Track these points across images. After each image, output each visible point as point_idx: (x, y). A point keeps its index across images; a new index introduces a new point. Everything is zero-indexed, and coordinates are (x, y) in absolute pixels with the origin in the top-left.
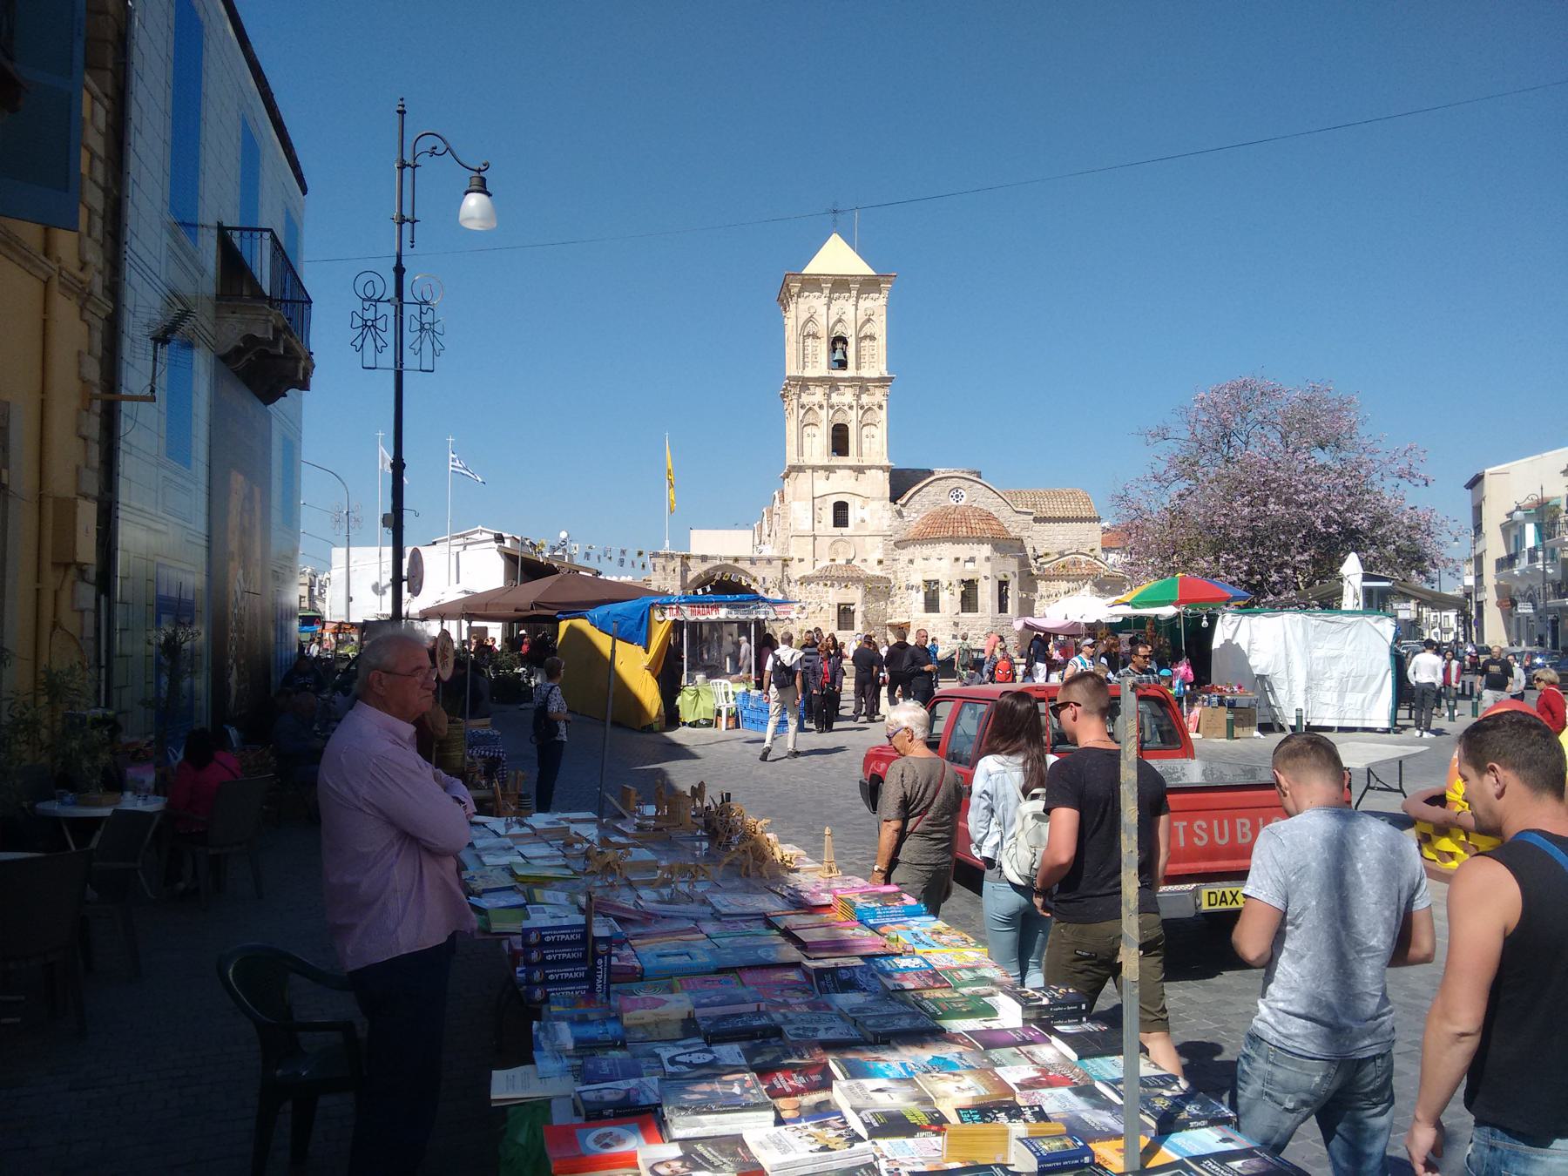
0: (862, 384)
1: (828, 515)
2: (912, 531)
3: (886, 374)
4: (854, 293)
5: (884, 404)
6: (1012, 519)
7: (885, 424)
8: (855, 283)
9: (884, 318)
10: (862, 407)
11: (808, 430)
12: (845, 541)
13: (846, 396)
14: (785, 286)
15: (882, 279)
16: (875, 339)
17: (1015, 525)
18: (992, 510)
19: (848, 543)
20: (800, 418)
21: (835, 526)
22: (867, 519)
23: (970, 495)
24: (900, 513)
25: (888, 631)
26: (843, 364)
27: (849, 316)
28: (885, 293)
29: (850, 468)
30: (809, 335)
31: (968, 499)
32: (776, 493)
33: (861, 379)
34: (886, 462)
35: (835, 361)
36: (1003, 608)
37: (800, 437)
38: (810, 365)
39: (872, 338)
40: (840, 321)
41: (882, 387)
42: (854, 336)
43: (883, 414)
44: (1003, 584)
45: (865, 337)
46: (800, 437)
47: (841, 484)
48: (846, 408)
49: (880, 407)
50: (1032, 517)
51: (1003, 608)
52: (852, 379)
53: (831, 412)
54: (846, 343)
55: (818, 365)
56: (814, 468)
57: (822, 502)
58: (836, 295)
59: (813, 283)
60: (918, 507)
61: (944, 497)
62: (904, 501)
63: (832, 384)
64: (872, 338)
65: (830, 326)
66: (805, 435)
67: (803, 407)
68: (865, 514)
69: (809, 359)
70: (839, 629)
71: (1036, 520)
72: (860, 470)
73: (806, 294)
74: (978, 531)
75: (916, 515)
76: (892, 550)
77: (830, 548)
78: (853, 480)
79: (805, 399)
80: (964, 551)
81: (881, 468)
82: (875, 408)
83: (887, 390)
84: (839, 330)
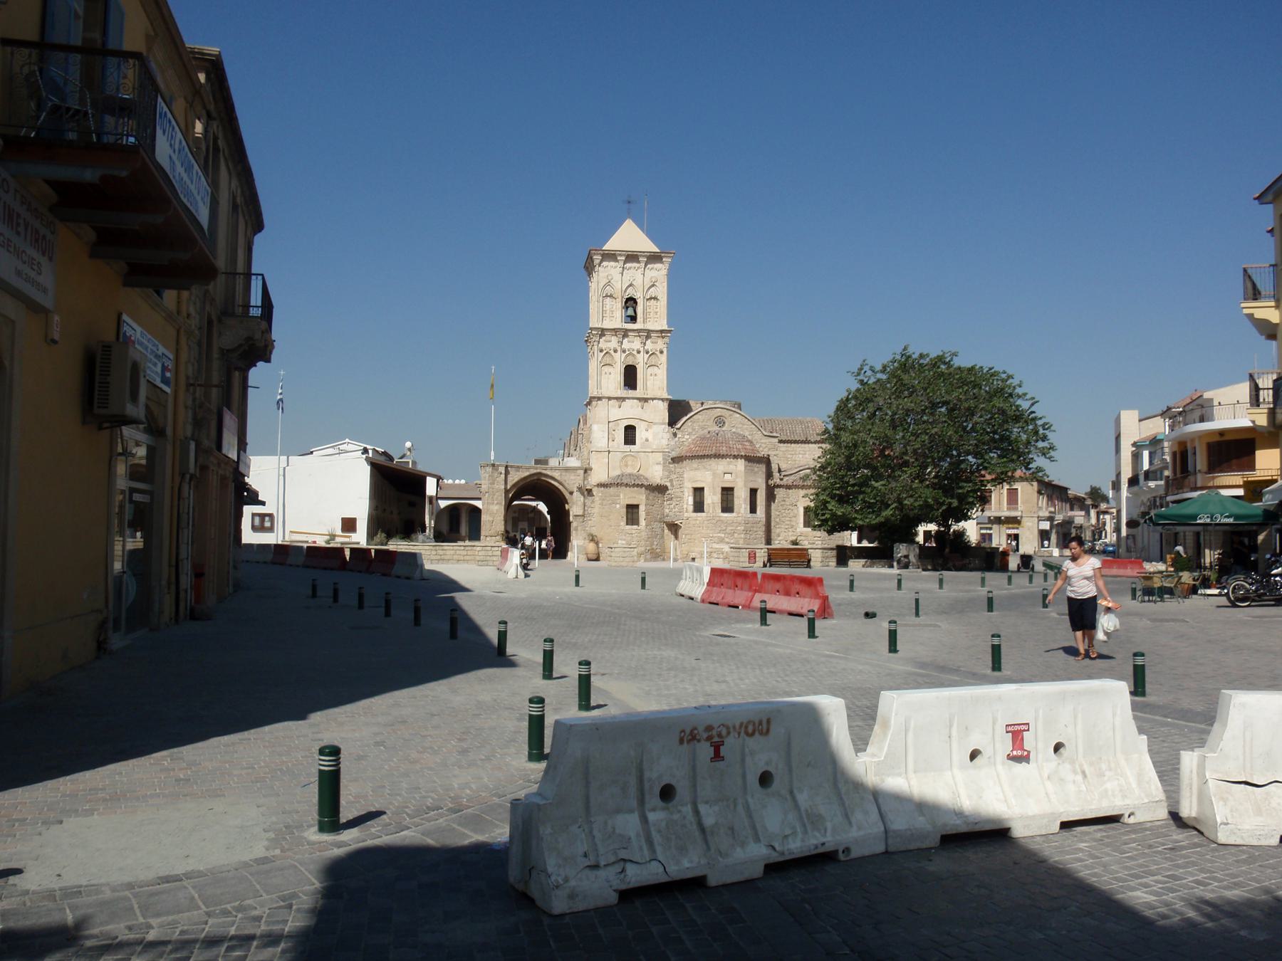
0: (648, 334)
1: (620, 435)
3: (666, 328)
6: (762, 441)
7: (665, 366)
10: (647, 353)
11: (606, 369)
12: (633, 456)
14: (590, 259)
15: (663, 255)
16: (658, 299)
17: (764, 446)
18: (747, 434)
24: (675, 435)
25: (665, 526)
26: (633, 319)
27: (638, 280)
28: (667, 265)
29: (639, 399)
30: (607, 296)
31: (729, 425)
33: (649, 332)
34: (666, 396)
35: (628, 316)
36: (753, 510)
37: (599, 374)
38: (608, 319)
39: (655, 298)
40: (631, 285)
41: (663, 337)
42: (642, 297)
43: (663, 358)
44: (753, 492)
45: (651, 298)
46: (599, 374)
47: (630, 411)
48: (635, 353)
49: (661, 352)
50: (776, 440)
51: (753, 510)
53: (624, 355)
55: (614, 319)
56: (610, 399)
58: (628, 265)
59: (611, 256)
60: (690, 430)
61: (711, 423)
62: (678, 426)
63: (625, 333)
64: (655, 298)
65: (624, 289)
67: (601, 351)
68: (649, 435)
70: (627, 524)
71: (781, 442)
75: (687, 437)
76: (669, 463)
77: (621, 461)
79: (603, 344)
80: (722, 465)
81: (663, 400)
82: (658, 353)
83: (666, 340)
84: (630, 292)
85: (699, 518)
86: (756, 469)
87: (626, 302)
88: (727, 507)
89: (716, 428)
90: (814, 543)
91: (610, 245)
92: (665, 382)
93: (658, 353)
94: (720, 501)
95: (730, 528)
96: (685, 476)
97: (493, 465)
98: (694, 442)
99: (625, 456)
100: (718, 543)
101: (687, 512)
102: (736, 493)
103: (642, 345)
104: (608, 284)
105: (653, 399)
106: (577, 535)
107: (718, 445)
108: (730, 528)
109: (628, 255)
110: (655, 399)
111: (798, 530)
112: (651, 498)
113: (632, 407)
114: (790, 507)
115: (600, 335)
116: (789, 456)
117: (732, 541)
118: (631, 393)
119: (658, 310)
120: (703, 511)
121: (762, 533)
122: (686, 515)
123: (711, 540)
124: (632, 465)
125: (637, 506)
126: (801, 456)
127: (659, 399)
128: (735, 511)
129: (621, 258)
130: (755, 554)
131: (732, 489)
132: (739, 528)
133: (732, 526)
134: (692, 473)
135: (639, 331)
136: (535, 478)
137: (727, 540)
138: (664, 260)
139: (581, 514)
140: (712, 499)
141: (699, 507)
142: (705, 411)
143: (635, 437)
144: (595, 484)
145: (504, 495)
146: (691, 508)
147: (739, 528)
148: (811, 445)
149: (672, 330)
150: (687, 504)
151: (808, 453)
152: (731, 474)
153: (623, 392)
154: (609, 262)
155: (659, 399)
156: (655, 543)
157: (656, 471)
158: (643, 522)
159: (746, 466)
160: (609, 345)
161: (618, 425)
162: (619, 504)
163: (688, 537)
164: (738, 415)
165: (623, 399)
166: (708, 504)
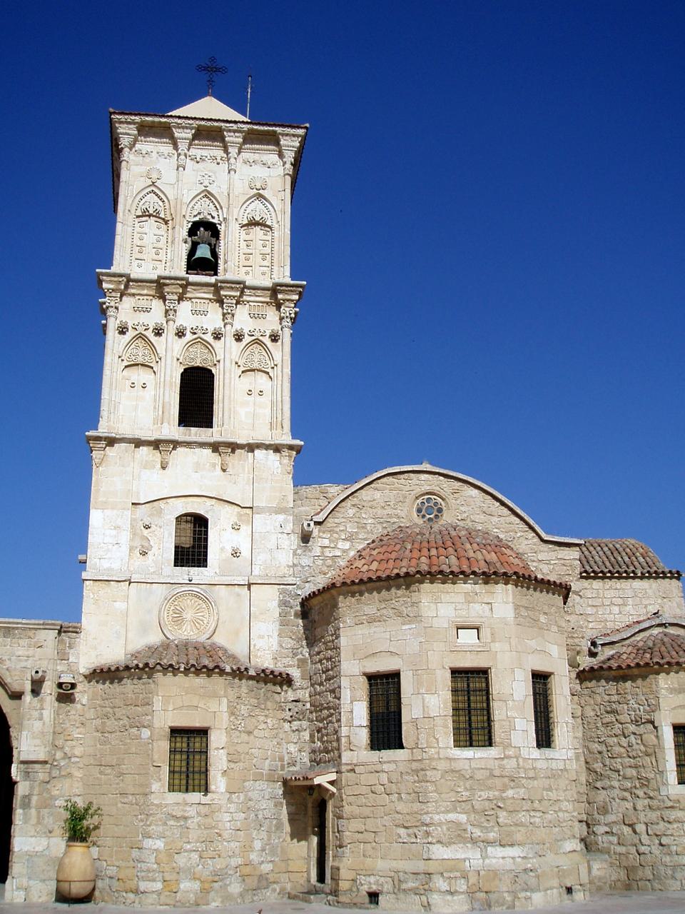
1: (165, 541)
7: (288, 370)
15: (279, 130)
19: (206, 600)
21: (175, 566)
26: (209, 266)
28: (290, 156)
29: (215, 447)
30: (146, 214)
34: (287, 439)
36: (544, 738)
43: (282, 353)
44: (541, 679)
45: (253, 223)
48: (209, 338)
50: (574, 554)
51: (544, 738)
56: (138, 443)
58: (196, 152)
60: (351, 528)
67: (122, 331)
75: (347, 545)
81: (277, 449)
82: (267, 340)
84: (205, 210)
85: (385, 767)
86: (543, 619)
87: (193, 231)
93: (267, 340)
95: (484, 795)
99: (177, 596)
102: (498, 686)
104: (153, 188)
105: (251, 448)
106: (26, 821)
107: (434, 552)
108: (484, 795)
110: (259, 446)
112: (244, 710)
113: (197, 467)
114: (632, 728)
116: (589, 610)
117: (492, 835)
118: (196, 434)
119: (267, 250)
120: (400, 746)
121: (570, 807)
122: (346, 757)
123: (428, 834)
124: (194, 622)
126: (616, 610)
127: (267, 447)
129: (184, 135)
132: (510, 793)
133: (490, 788)
134: (361, 630)
135: (216, 288)
137: (477, 833)
139: (42, 757)
142: (390, 479)
144: (87, 672)
146: (363, 736)
147: (510, 793)
148: (637, 584)
151: (630, 601)
153: (172, 430)
155: (267, 447)
156: (258, 845)
157: (261, 637)
158: (218, 782)
159: (517, 607)
160: (143, 318)
165: (176, 444)
166: (415, 722)
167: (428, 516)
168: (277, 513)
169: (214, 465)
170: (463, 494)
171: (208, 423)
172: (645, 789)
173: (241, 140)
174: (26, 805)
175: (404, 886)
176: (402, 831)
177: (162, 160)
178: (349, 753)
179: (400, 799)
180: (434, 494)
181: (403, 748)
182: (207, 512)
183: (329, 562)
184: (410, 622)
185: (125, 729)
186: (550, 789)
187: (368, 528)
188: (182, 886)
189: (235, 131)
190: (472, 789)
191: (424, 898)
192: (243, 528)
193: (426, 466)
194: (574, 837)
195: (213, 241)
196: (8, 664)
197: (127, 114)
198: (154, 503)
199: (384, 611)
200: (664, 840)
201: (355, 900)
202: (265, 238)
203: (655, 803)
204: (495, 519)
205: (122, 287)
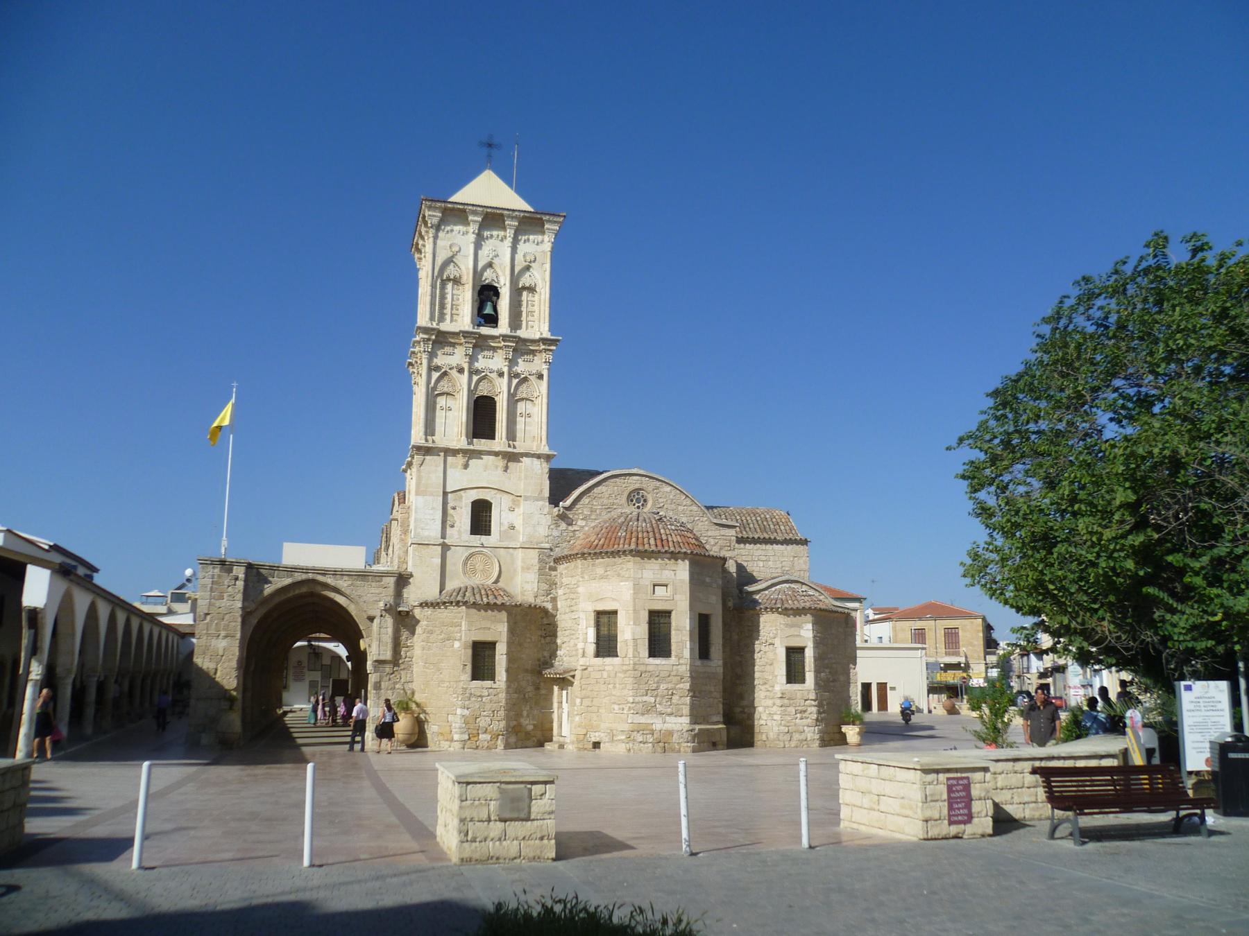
1: (463, 518)
2: (578, 544)
3: (547, 335)
4: (510, 233)
5: (545, 373)
6: (709, 533)
7: (545, 400)
8: (513, 218)
9: (548, 266)
13: (494, 362)
17: (717, 541)
18: (684, 520)
20: (432, 384)
22: (518, 523)
23: (655, 501)
26: (492, 320)
29: (496, 454)
31: (654, 505)
32: (396, 495)
34: (545, 450)
39: (531, 289)
40: (490, 265)
43: (541, 389)
48: (494, 375)
50: (732, 532)
52: (505, 338)
54: (497, 294)
56: (449, 452)
57: (455, 500)
58: (486, 233)
59: (458, 214)
62: (569, 502)
63: (481, 344)
64: (531, 289)
66: (438, 407)
69: (448, 311)
71: (741, 540)
72: (512, 457)
73: (448, 228)
74: (671, 544)
78: (500, 471)
80: (652, 570)
81: (539, 456)
83: (550, 357)
84: (488, 276)
86: (708, 580)
88: (658, 644)
89: (631, 510)
90: (805, 711)
91: (460, 197)
92: (544, 427)
94: (647, 637)
96: (580, 590)
97: (222, 563)
98: (598, 529)
99: (472, 555)
100: (643, 714)
101: (583, 656)
103: (507, 363)
109: (487, 213)
111: (778, 688)
113: (486, 468)
115: (434, 342)
117: (669, 710)
125: (492, 645)
126: (761, 564)
128: (673, 653)
130: (967, 788)
131: (667, 614)
132: (681, 686)
136: (304, 590)
138: (546, 226)
140: (631, 632)
141: (606, 645)
143: (490, 521)
145: (239, 620)
146: (591, 648)
149: (558, 340)
150: (585, 641)
151: (772, 558)
152: (666, 586)
154: (455, 225)
161: (461, 497)
162: (460, 640)
163: (586, 702)
164: (668, 489)
167: (637, 505)
168: (537, 500)
169: (497, 467)
170: (662, 490)
171: (491, 436)
172: (767, 686)
173: (517, 224)
174: (378, 686)
175: (615, 739)
176: (616, 707)
177: (459, 236)
178: (584, 659)
179: (614, 687)
180: (643, 490)
181: (617, 656)
182: (492, 498)
183: (571, 534)
184: (625, 581)
185: (443, 640)
186: (706, 685)
187: (598, 512)
188: (481, 736)
189: (513, 218)
190: (658, 683)
191: (627, 745)
192: (516, 510)
193: (635, 471)
194: (719, 713)
195: (495, 298)
196: (365, 598)
197: (435, 201)
198: (458, 493)
199: (608, 573)
200: (775, 717)
201: (585, 746)
202: (533, 299)
203: (772, 694)
204: (681, 508)
205: (434, 337)
